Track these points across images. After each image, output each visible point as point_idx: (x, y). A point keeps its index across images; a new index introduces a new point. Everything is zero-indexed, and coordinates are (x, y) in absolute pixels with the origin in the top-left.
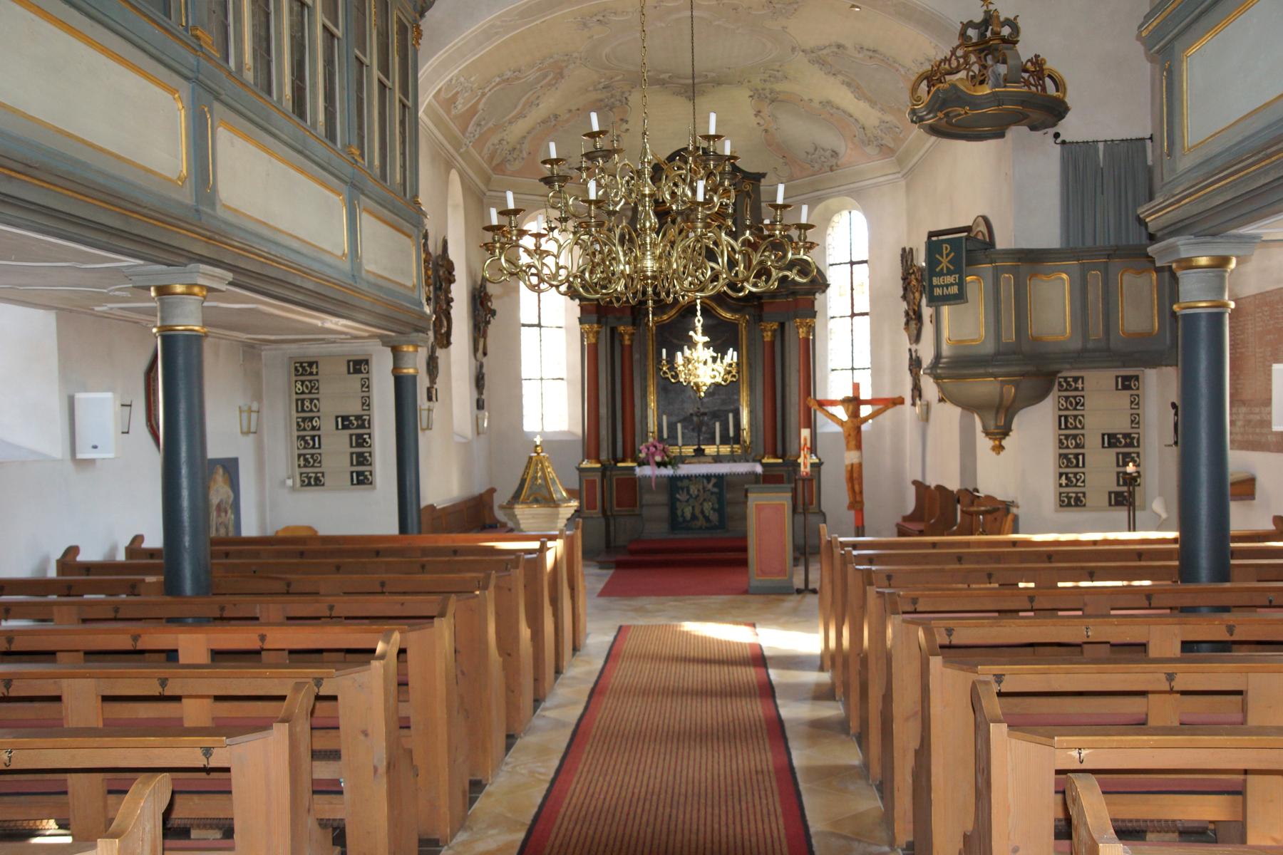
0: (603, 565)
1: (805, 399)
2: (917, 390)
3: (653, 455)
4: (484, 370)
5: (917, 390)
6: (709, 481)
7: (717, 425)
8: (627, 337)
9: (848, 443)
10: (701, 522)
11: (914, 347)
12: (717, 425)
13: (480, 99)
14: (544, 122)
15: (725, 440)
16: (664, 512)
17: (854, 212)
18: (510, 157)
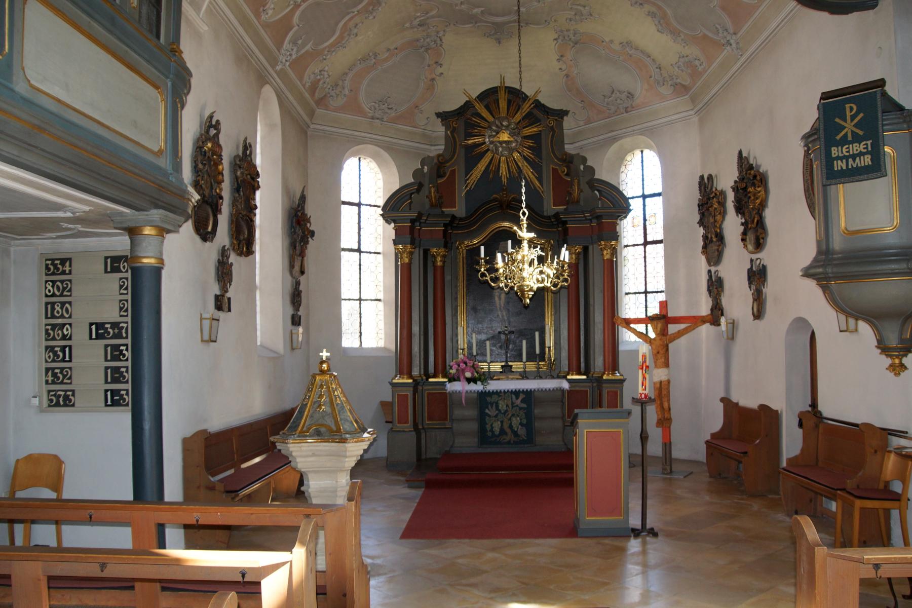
0: (411, 484)
2: (717, 311)
3: (463, 371)
4: (301, 288)
5: (717, 311)
6: (517, 398)
7: (524, 342)
8: (439, 259)
10: (510, 437)
11: (713, 269)
12: (524, 342)
13: (293, 11)
14: (364, 59)
15: (531, 357)
16: (474, 426)
17: (646, 152)
18: (332, 93)
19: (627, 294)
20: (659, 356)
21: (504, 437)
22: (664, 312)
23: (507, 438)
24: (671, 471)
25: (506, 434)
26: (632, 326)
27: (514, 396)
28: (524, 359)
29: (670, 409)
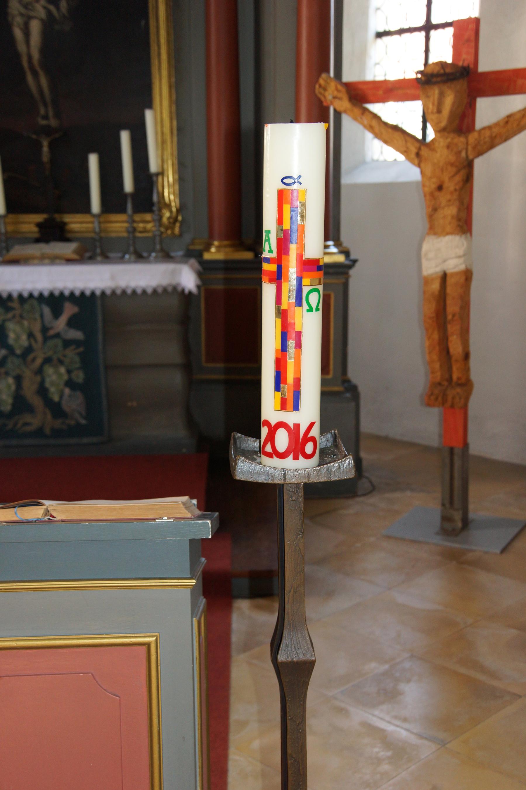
1: (313, 80)
9: (433, 211)
10: (38, 419)
19: (379, 35)
20: (443, 198)
21: (28, 418)
22: (467, 59)
23: (34, 421)
24: (466, 523)
25: (30, 409)
26: (375, 108)
27: (47, 311)
28: (96, 205)
29: (467, 356)
